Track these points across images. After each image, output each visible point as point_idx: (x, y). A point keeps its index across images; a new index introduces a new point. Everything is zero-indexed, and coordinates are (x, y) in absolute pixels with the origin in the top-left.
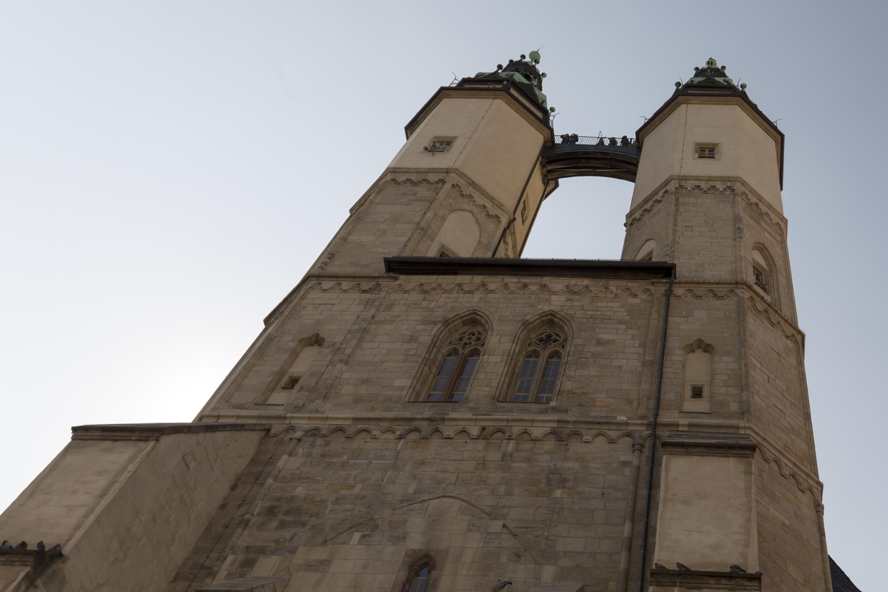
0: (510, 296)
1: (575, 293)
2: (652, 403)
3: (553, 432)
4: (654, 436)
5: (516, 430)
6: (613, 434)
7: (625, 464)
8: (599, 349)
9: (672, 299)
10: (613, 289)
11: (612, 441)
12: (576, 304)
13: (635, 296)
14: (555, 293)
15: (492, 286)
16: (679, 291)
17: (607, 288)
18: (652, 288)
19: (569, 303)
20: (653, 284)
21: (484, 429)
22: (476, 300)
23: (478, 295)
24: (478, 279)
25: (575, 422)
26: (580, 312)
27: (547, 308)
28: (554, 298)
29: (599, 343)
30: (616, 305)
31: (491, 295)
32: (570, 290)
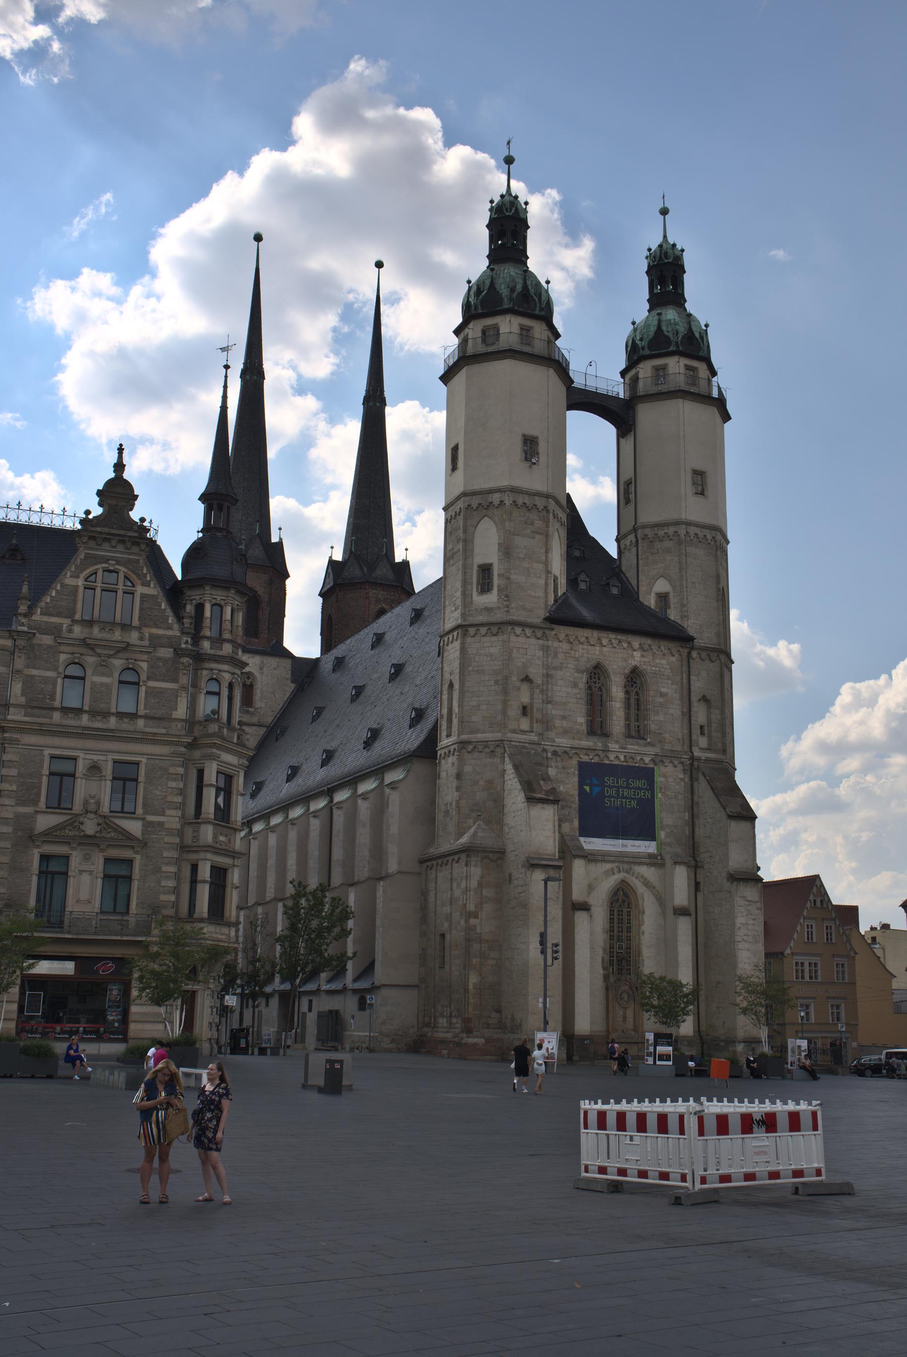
0: (614, 650)
1: (645, 651)
2: (687, 742)
3: (652, 760)
4: (692, 765)
5: (638, 758)
6: (676, 762)
7: (682, 779)
8: (661, 700)
9: (691, 661)
10: (663, 648)
11: (675, 767)
12: (646, 660)
13: (673, 656)
14: (635, 650)
15: (605, 642)
16: (694, 654)
17: (659, 647)
18: (681, 649)
19: (643, 659)
20: (682, 647)
21: (625, 756)
22: (598, 653)
23: (597, 648)
24: (596, 634)
25: (661, 756)
26: (649, 668)
27: (634, 663)
28: (635, 653)
29: (662, 695)
30: (664, 662)
31: (605, 649)
32: (641, 648)
